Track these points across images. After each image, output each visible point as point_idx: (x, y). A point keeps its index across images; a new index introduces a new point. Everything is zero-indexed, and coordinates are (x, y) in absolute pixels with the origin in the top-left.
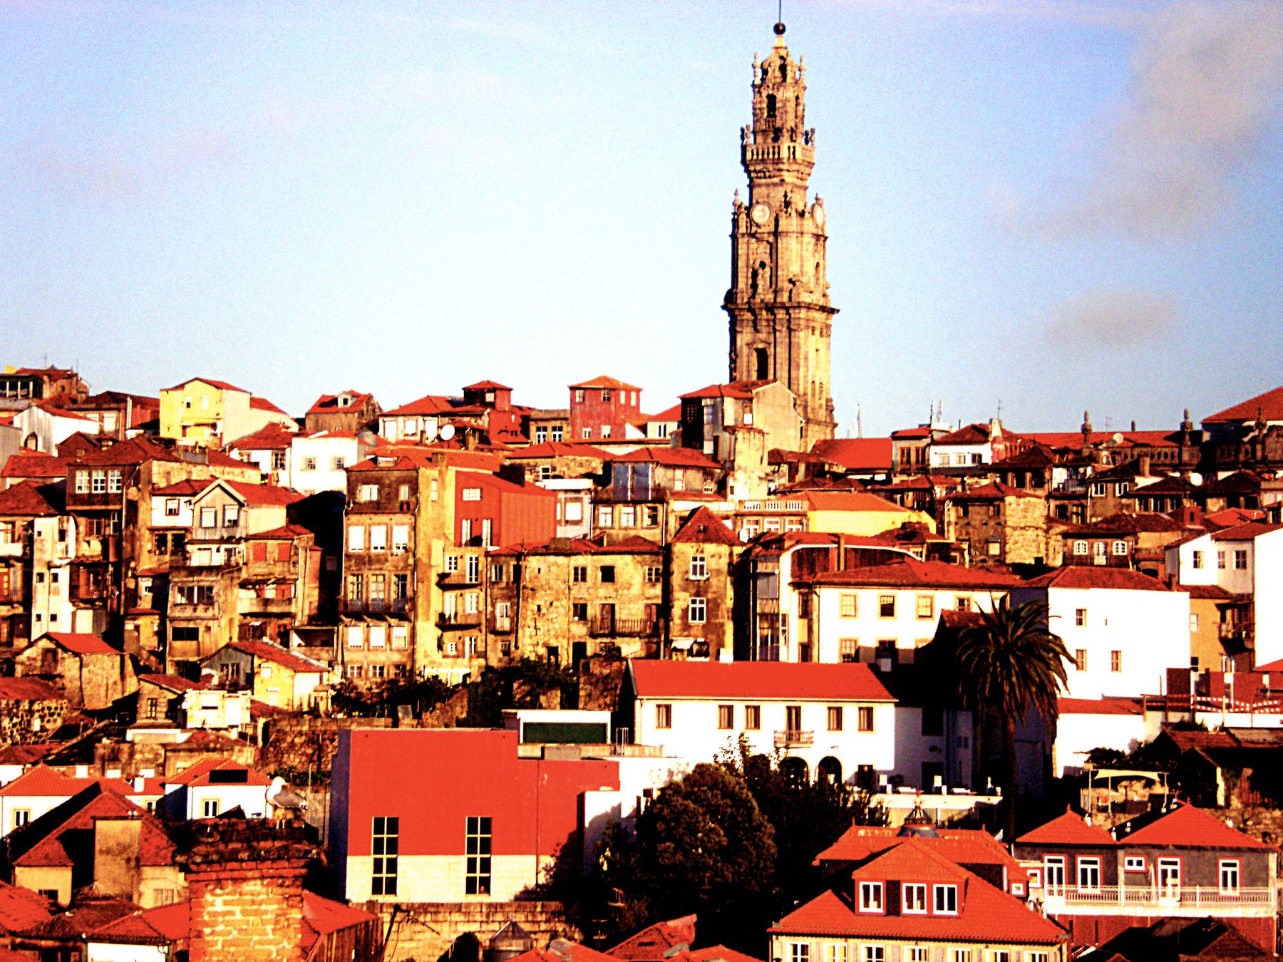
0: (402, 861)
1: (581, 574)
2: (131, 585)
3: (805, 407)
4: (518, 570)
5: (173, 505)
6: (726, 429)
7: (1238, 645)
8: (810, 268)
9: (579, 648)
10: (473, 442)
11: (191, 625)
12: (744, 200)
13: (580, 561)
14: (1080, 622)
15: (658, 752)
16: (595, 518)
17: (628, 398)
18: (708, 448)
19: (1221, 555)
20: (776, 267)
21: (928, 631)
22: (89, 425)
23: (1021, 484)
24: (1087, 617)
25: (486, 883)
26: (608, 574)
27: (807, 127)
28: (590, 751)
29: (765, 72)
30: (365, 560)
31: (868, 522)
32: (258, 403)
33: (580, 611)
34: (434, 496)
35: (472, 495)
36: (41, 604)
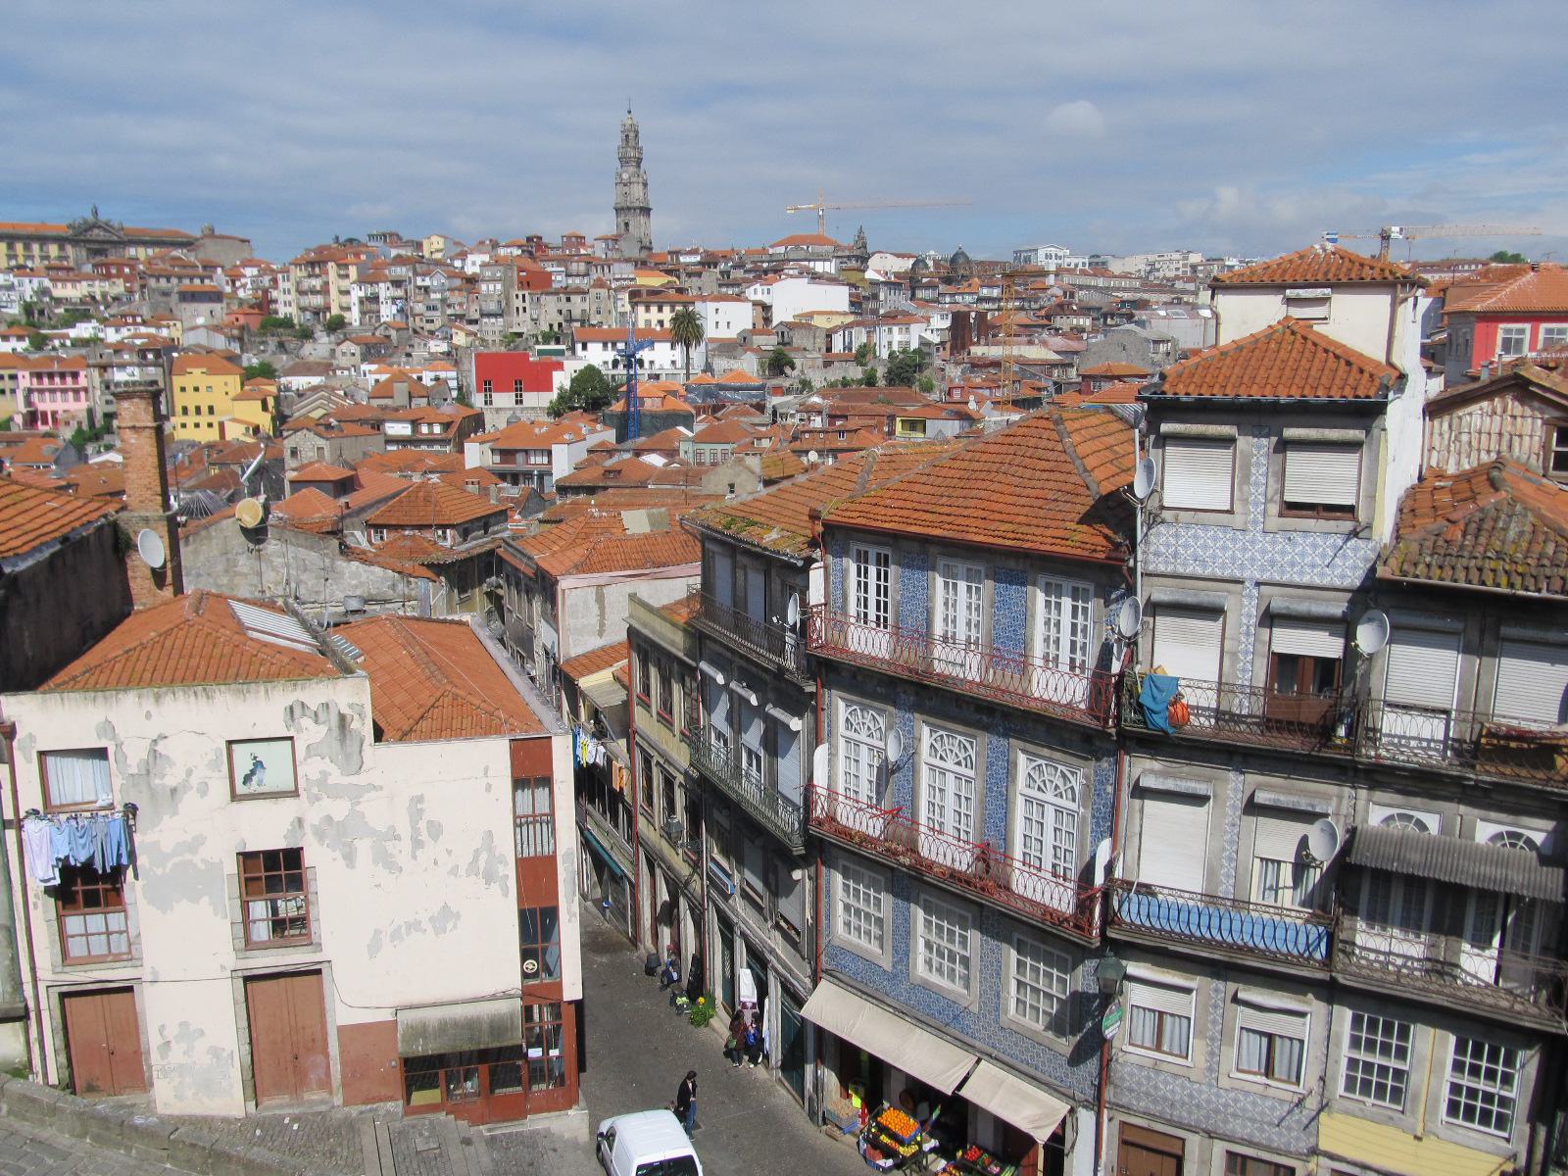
7: (767, 320)
9: (560, 325)
15: (580, 359)
22: (402, 252)
26: (568, 300)
28: (559, 358)
30: (488, 296)
31: (656, 281)
32: (457, 244)
33: (560, 312)
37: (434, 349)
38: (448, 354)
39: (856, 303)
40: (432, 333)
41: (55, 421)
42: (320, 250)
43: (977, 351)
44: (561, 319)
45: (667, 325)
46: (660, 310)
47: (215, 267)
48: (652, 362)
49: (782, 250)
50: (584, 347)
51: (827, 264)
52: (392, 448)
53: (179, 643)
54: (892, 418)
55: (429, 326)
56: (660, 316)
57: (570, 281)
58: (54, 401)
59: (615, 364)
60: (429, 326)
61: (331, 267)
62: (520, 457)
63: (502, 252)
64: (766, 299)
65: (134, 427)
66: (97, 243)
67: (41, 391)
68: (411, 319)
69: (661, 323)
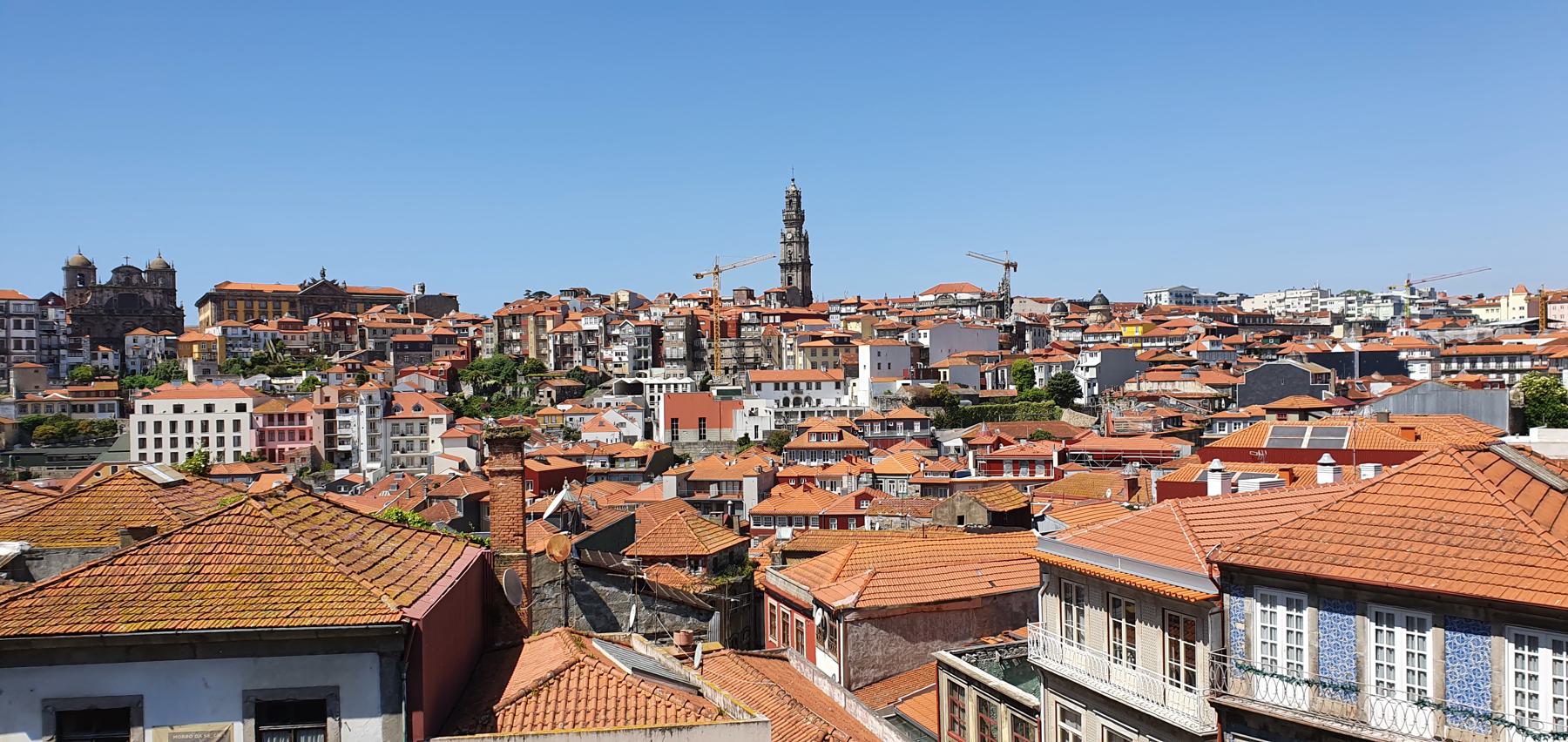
7: (926, 361)
41: (282, 457)
42: (520, 303)
43: (1131, 387)
46: (825, 354)
47: (423, 322)
49: (931, 298)
50: (759, 388)
53: (573, 684)
55: (616, 370)
58: (281, 440)
59: (786, 402)
60: (616, 370)
61: (531, 318)
62: (713, 489)
63: (680, 304)
64: (925, 342)
65: (502, 473)
66: (324, 297)
67: (272, 432)
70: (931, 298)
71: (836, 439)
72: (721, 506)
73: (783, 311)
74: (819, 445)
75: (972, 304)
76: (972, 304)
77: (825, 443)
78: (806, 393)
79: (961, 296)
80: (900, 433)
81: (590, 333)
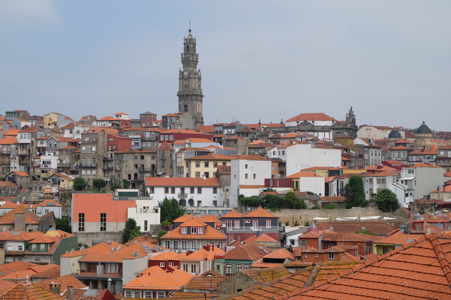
0: (85, 223)
1: (136, 158)
2: (33, 160)
3: (196, 118)
4: (122, 157)
5: (42, 142)
6: (172, 124)
7: (283, 173)
8: (197, 86)
9: (136, 175)
10: (116, 127)
11: (46, 170)
12: (182, 70)
13: (136, 155)
14: (246, 168)
16: (142, 145)
17: (154, 117)
18: (168, 128)
19: (279, 152)
20: (189, 86)
21: (215, 170)
22: (29, 124)
23: (243, 136)
24: (248, 166)
25: (105, 229)
26: (142, 158)
27: (196, 53)
29: (186, 40)
30: (86, 154)
33: (136, 166)
34: (102, 140)
35: (111, 140)
36: (12, 165)
37: (46, 191)
38: (57, 194)
39: (347, 160)
40: (45, 179)
44: (136, 171)
45: (211, 176)
46: (207, 165)
48: (199, 202)
51: (327, 134)
52: (10, 260)
54: (370, 244)
55: (43, 175)
56: (207, 170)
57: (144, 145)
60: (43, 175)
62: (99, 268)
63: (99, 124)
68: (31, 170)
69: (207, 174)
70: (294, 124)
71: (200, 232)
72: (105, 282)
73: (176, 131)
74: (189, 236)
75: (324, 129)
76: (324, 129)
77: (193, 235)
78: (189, 196)
79: (318, 123)
80: (254, 229)
81: (23, 145)
